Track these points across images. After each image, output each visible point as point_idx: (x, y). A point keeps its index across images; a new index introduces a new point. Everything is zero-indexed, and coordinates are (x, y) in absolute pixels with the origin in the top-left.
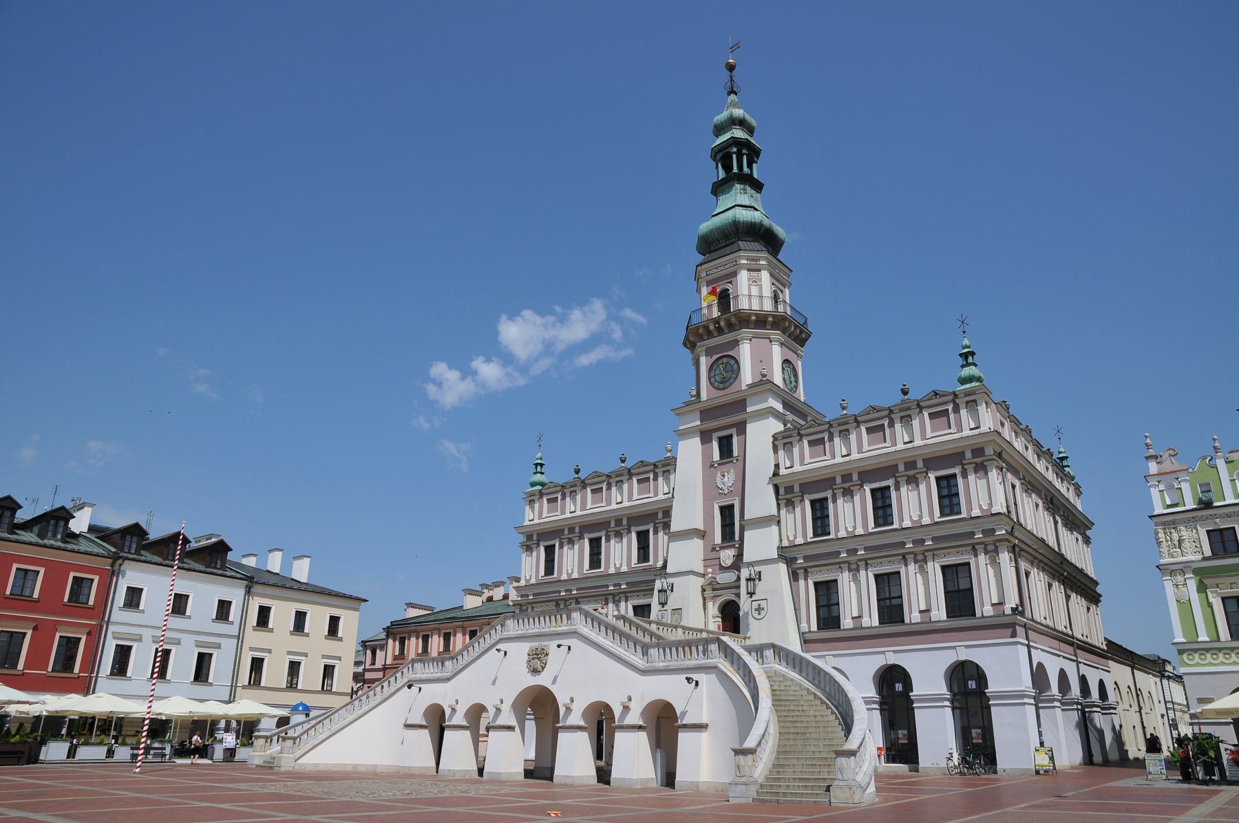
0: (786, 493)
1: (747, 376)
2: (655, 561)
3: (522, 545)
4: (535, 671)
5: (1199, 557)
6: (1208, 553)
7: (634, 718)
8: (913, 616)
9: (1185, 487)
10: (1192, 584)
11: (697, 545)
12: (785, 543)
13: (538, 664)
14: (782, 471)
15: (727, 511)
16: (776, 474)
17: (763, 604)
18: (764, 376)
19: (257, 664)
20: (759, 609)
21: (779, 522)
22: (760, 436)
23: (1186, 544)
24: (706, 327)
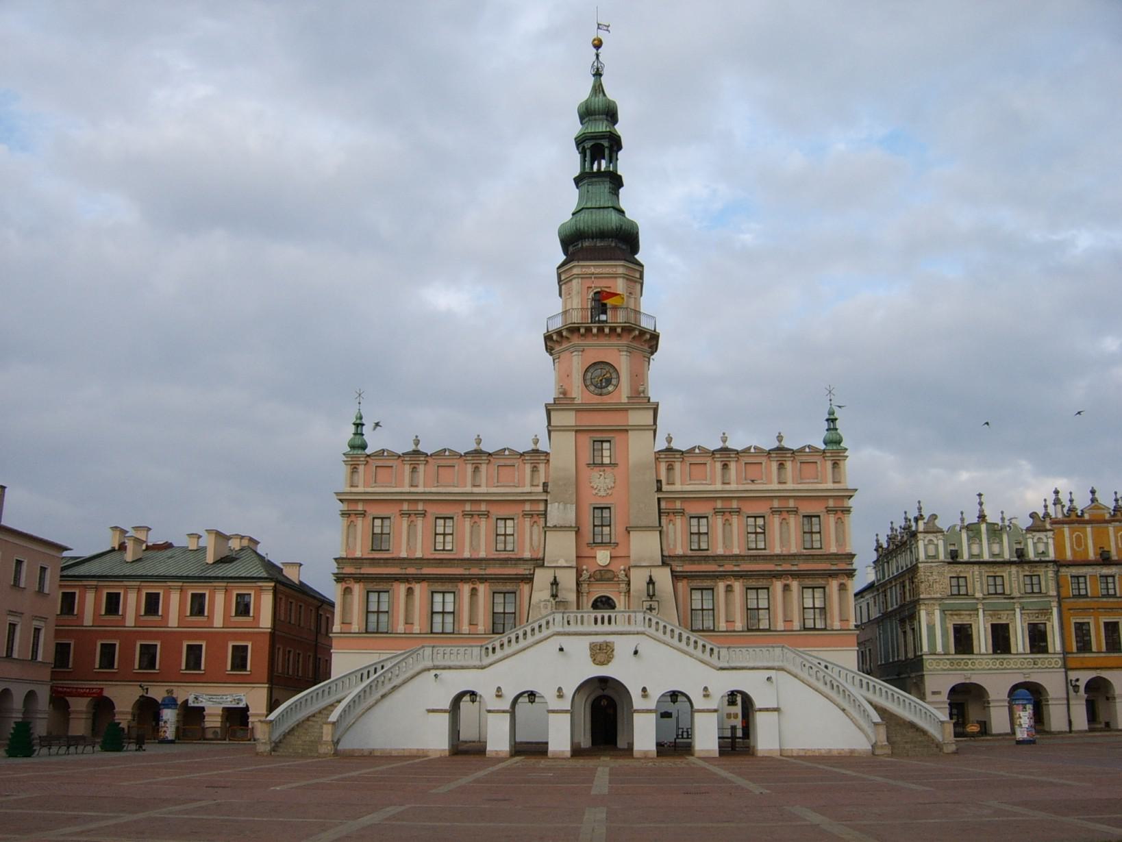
3: (344, 514)
7: (652, 704)
9: (941, 543)
10: (937, 613)
12: (666, 553)
13: (600, 657)
14: (665, 488)
16: (659, 490)
17: (655, 605)
24: (589, 330)
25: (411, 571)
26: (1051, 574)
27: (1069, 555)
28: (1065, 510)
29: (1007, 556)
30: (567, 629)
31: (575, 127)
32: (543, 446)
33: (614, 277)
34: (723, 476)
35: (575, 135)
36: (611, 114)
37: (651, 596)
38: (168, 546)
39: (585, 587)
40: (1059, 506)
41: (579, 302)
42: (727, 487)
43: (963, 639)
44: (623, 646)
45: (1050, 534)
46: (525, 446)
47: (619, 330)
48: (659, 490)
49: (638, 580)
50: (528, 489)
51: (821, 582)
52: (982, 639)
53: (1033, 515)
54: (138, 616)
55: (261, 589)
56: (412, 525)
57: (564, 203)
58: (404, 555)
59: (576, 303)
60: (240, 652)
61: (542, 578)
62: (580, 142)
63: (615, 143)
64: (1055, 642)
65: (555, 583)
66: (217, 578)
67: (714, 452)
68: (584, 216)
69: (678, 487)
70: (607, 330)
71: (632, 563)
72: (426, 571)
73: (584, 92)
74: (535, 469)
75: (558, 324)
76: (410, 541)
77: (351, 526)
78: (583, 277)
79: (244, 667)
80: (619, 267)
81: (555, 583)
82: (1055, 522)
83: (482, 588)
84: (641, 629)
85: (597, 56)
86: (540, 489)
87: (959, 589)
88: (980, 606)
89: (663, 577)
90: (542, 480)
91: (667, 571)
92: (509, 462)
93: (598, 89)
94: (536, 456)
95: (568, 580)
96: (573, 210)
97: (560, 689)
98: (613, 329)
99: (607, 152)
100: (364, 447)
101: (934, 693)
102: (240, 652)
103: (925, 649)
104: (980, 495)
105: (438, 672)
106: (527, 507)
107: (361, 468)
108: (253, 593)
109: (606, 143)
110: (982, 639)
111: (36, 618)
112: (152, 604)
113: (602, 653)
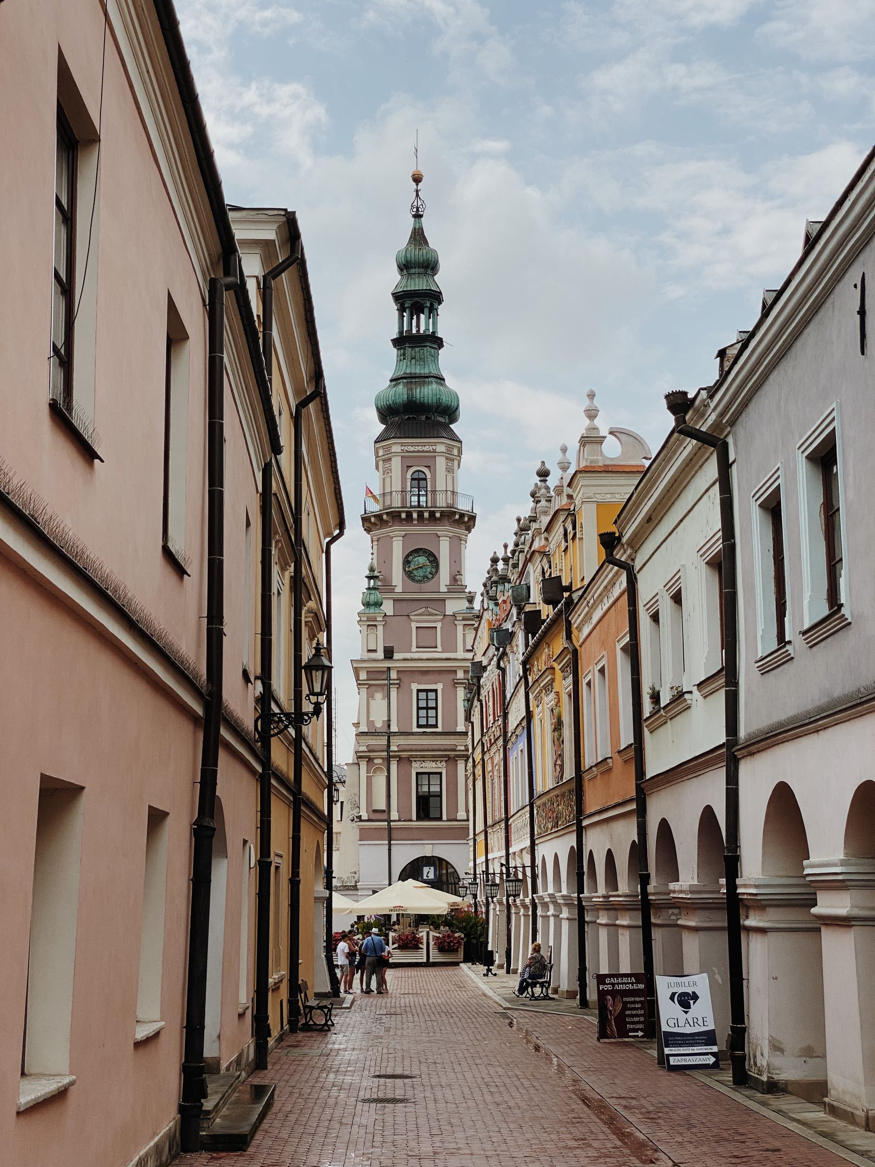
24: (409, 515)
35: (392, 289)
36: (430, 266)
47: (438, 515)
62: (400, 298)
70: (426, 515)
80: (441, 446)
85: (417, 191)
96: (390, 375)
99: (426, 311)
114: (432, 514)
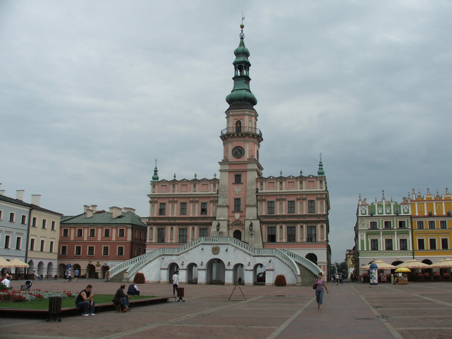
0: (260, 198)
1: (247, 156)
2: (210, 214)
3: (151, 202)
4: (216, 254)
5: (367, 229)
6: (370, 228)
8: (298, 240)
9: (367, 210)
10: (365, 235)
11: (226, 209)
12: (259, 215)
14: (259, 191)
15: (237, 200)
16: (257, 192)
17: (253, 233)
18: (253, 157)
19: (33, 240)
20: (252, 235)
21: (257, 207)
22: (251, 177)
23: (365, 225)
24: (233, 135)
25: (172, 221)
26: (409, 220)
27: (417, 214)
28: (417, 196)
29: (392, 214)
30: (205, 242)
31: (233, 58)
32: (218, 177)
33: (244, 115)
34: (280, 187)
36: (247, 54)
37: (251, 230)
38: (103, 212)
39: (230, 227)
40: (414, 195)
41: (233, 124)
42: (281, 191)
43: (375, 245)
44: (222, 249)
45: (410, 205)
46: (211, 177)
48: (257, 192)
49: (247, 224)
50: (212, 192)
51: (314, 225)
52: (382, 245)
53: (404, 198)
54: (88, 237)
55: (127, 227)
56: (173, 206)
57: (228, 87)
58: (170, 216)
59: (231, 125)
60: (121, 249)
61: (215, 223)
62: (235, 64)
63: (247, 65)
64: (410, 247)
65: (218, 225)
66: (113, 224)
67: (277, 178)
68: (234, 93)
69: (264, 191)
70: (240, 135)
71: (246, 218)
72: (177, 221)
73: (236, 46)
74: (215, 186)
75: (225, 132)
76: (173, 211)
77: (153, 207)
78: (233, 116)
79: (122, 254)
81: (218, 225)
82: (412, 201)
83: (196, 228)
84: (228, 243)
85: (242, 31)
86: (216, 192)
87: (374, 225)
88: (381, 233)
89: (257, 224)
90: (217, 189)
91: (258, 222)
92: (205, 183)
93: (242, 44)
94: (215, 181)
95: (224, 225)
96: (232, 90)
97: (202, 262)
98: (242, 135)
100: (158, 179)
101: (362, 265)
102: (121, 249)
103: (360, 249)
104: (383, 191)
105: (163, 257)
106: (212, 199)
107: (156, 186)
108: (125, 229)
109: (243, 65)
110: (382, 245)
111: (51, 238)
112: (92, 233)
113: (216, 251)
114: (242, 135)
